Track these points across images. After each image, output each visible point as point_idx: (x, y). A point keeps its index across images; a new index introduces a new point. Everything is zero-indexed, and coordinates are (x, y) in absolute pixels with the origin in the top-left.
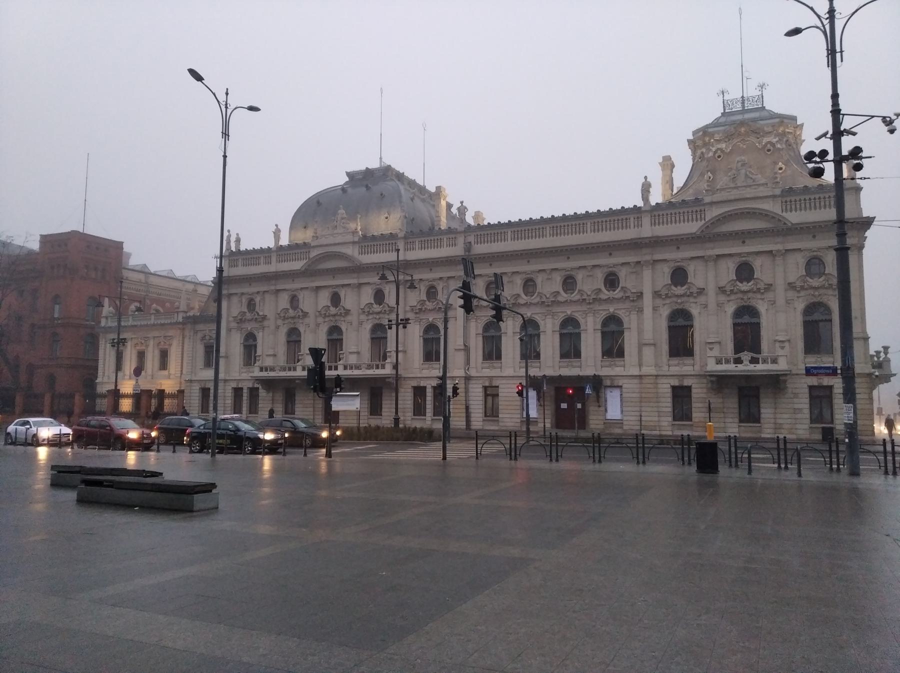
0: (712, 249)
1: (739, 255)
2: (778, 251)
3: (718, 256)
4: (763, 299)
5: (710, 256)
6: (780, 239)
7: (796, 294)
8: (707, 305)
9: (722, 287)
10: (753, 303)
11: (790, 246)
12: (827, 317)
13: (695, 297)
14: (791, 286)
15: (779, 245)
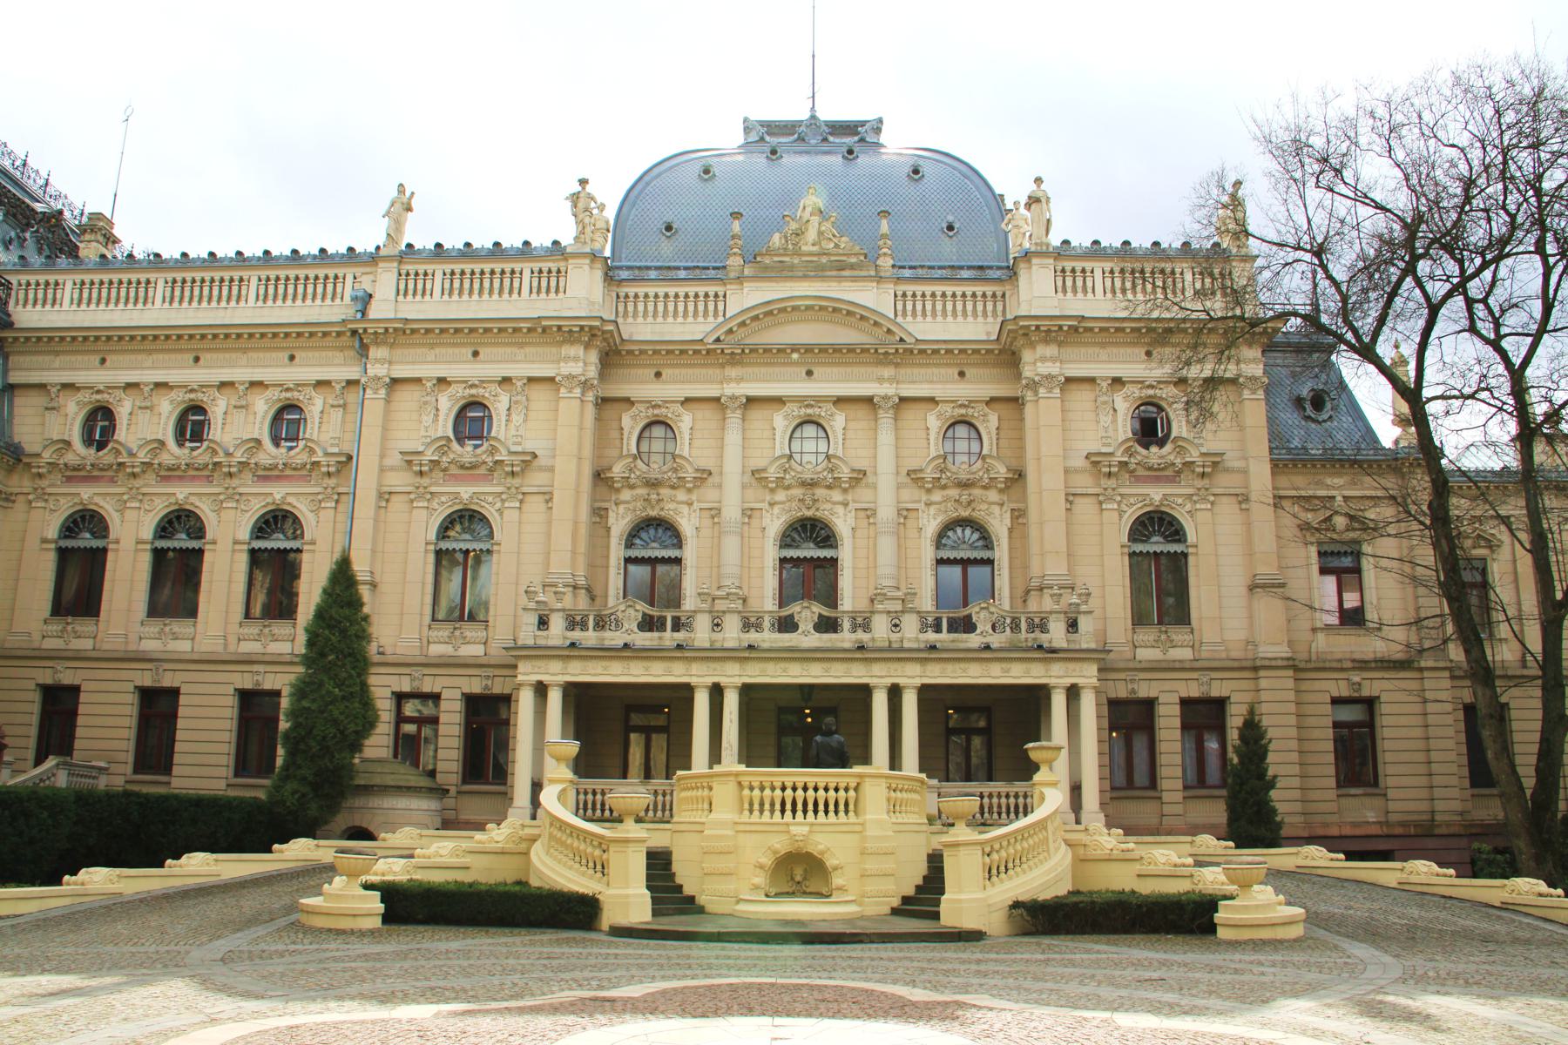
0: (740, 380)
1: (801, 400)
2: (886, 398)
3: (751, 401)
4: (846, 505)
5: (733, 398)
6: (888, 372)
7: (924, 498)
8: (720, 510)
9: (758, 471)
10: (823, 511)
11: (909, 391)
12: (985, 554)
13: (689, 491)
14: (915, 477)
15: (886, 385)
